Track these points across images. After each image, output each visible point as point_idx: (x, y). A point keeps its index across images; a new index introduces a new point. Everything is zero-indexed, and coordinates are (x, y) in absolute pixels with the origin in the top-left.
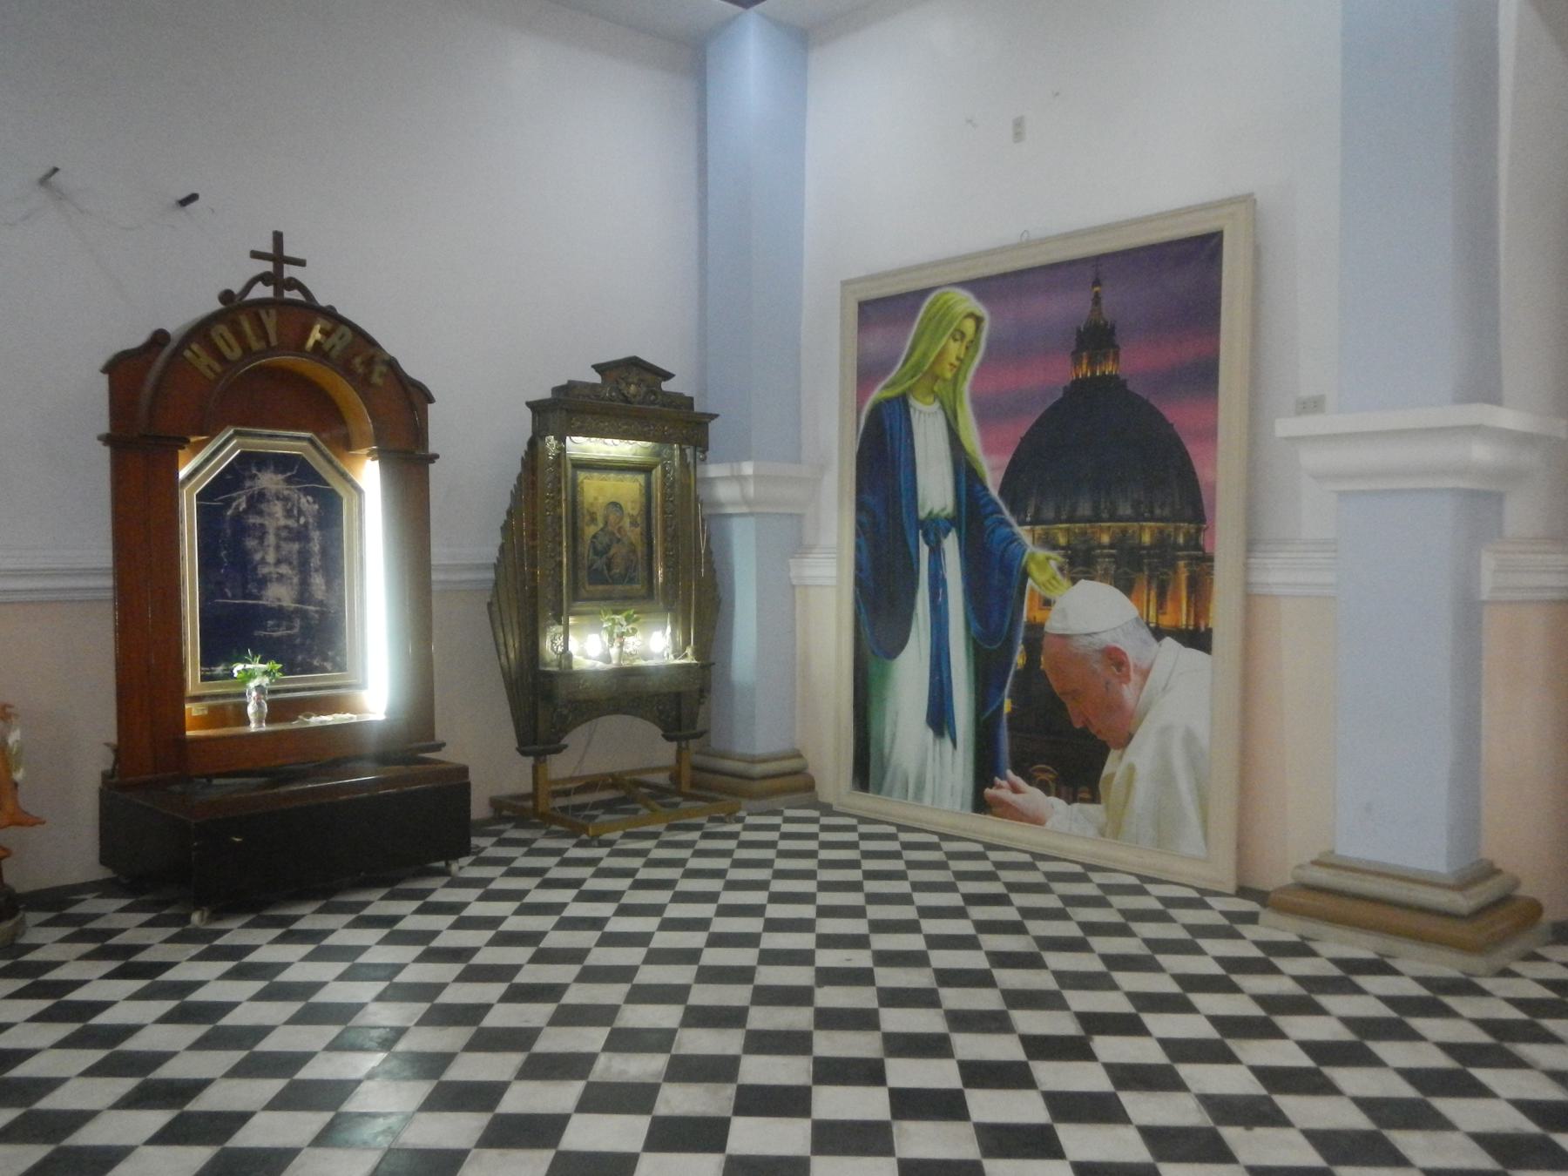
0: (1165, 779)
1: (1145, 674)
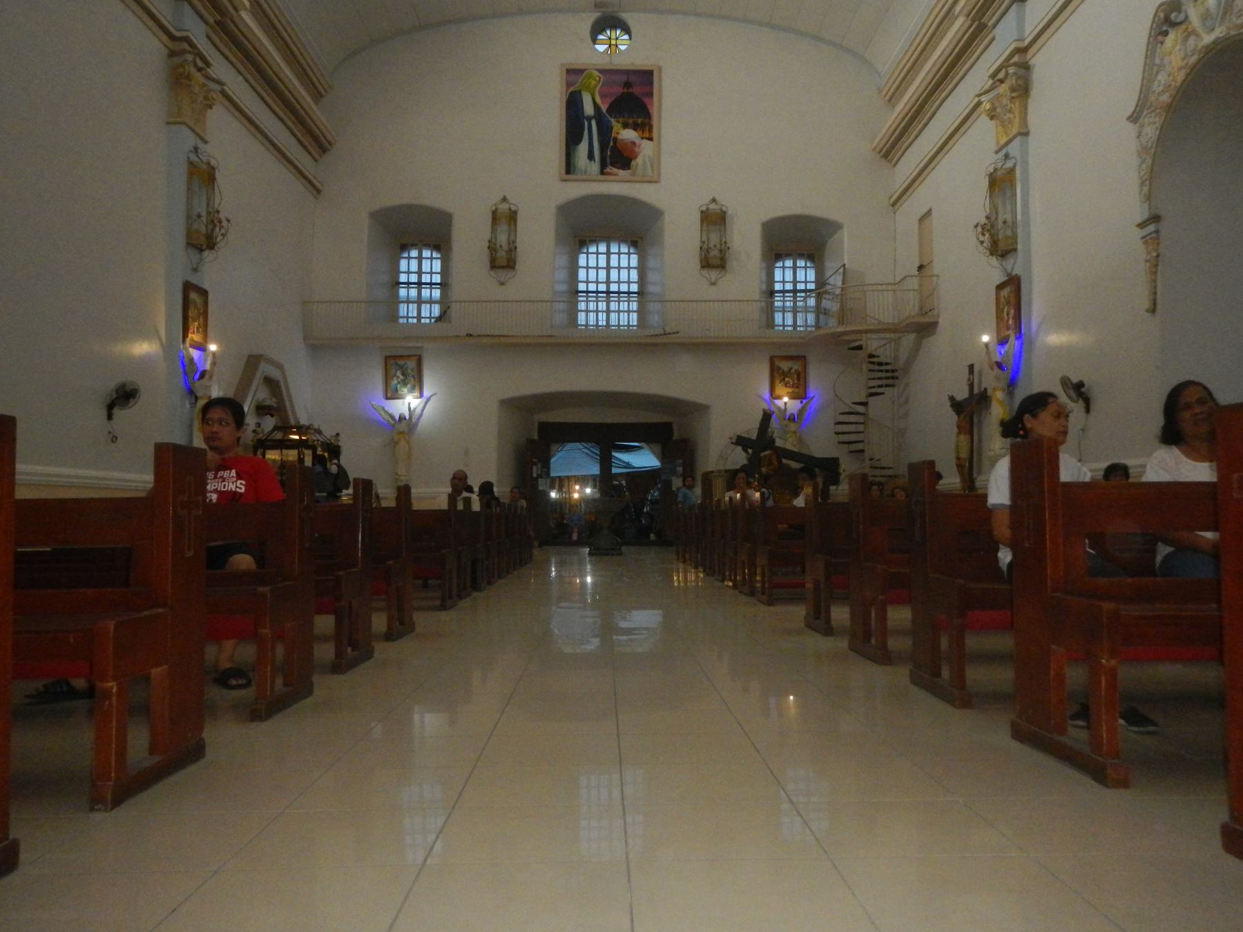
0: (644, 161)
1: (640, 146)
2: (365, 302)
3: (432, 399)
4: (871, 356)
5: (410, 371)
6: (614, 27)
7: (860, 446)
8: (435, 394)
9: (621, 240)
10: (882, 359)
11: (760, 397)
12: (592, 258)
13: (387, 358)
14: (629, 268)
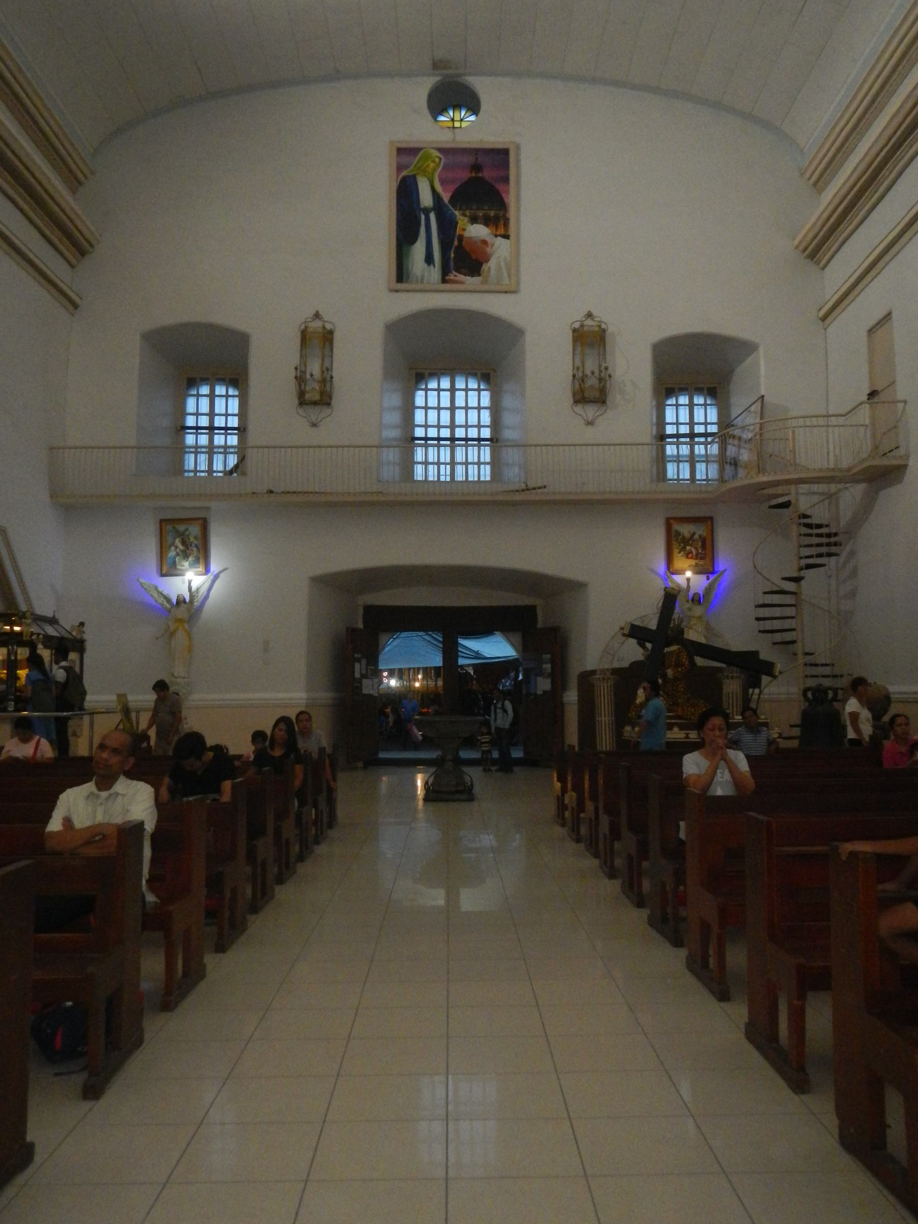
1: (493, 245)
2: (133, 448)
3: (221, 575)
4: (805, 516)
5: (192, 539)
6: (457, 106)
7: (788, 636)
8: (226, 569)
9: (469, 373)
10: (814, 521)
11: (652, 571)
12: (432, 395)
13: (162, 521)
14: (479, 408)
